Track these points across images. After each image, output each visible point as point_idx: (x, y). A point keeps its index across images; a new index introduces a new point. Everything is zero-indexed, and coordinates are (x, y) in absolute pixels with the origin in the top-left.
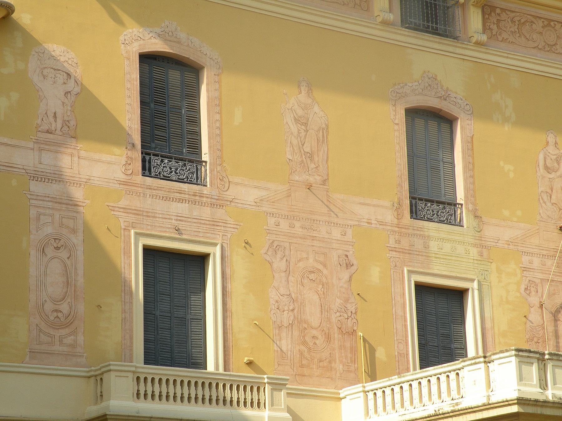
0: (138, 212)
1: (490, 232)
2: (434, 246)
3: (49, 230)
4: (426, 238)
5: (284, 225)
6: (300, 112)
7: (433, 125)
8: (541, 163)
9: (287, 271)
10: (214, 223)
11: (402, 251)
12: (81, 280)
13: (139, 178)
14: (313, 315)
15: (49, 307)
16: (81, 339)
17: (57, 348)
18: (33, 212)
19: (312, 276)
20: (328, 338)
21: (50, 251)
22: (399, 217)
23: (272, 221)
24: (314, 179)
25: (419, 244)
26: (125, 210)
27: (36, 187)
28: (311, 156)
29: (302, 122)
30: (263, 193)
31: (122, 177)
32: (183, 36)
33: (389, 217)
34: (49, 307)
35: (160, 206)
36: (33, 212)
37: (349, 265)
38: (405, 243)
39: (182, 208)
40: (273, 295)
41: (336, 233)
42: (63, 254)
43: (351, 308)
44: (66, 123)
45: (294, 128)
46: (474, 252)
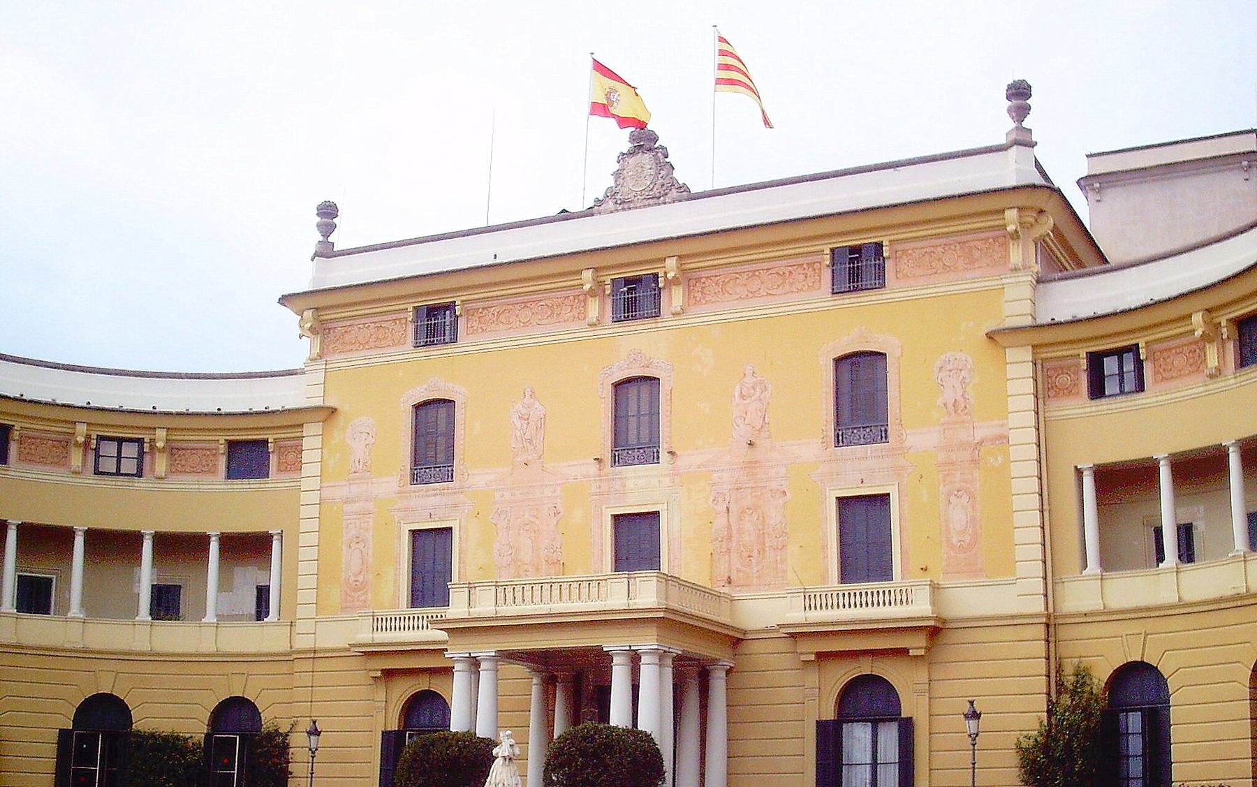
0: (406, 509)
1: (681, 462)
2: (630, 484)
6: (524, 411)
8: (737, 394)
11: (601, 494)
12: (371, 560)
15: (353, 578)
16: (370, 596)
18: (344, 525)
19: (527, 527)
23: (498, 494)
28: (530, 441)
29: (525, 418)
33: (593, 469)
36: (344, 525)
41: (548, 492)
46: (667, 481)
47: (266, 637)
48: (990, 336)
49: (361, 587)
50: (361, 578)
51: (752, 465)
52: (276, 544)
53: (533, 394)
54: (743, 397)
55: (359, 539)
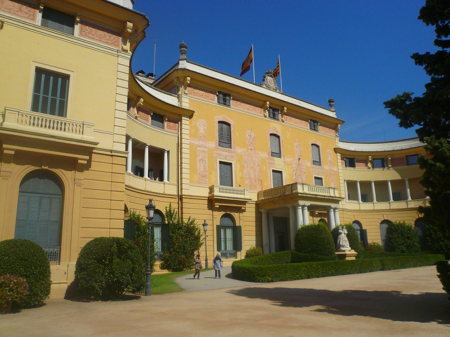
0: (218, 154)
1: (286, 159)
2: (276, 162)
3: (201, 157)
4: (274, 161)
5: (247, 157)
7: (275, 137)
9: (247, 167)
10: (233, 157)
12: (207, 168)
13: (218, 147)
14: (252, 176)
17: (203, 182)
20: (256, 181)
21: (201, 162)
22: (269, 156)
24: (252, 148)
25: (273, 162)
26: (215, 153)
27: (198, 148)
28: (252, 143)
30: (242, 151)
31: (215, 146)
32: (226, 118)
33: (267, 156)
34: (201, 173)
35: (222, 153)
36: (198, 154)
37: (259, 166)
38: (270, 161)
39: (227, 153)
40: (245, 172)
42: (204, 162)
43: (260, 175)
44: (204, 135)
45: (248, 137)
46: (283, 163)
47: (168, 187)
48: (334, 149)
49: (205, 176)
50: (204, 173)
51: (299, 164)
52: (166, 155)
53: (251, 130)
54: (297, 147)
55: (203, 160)
